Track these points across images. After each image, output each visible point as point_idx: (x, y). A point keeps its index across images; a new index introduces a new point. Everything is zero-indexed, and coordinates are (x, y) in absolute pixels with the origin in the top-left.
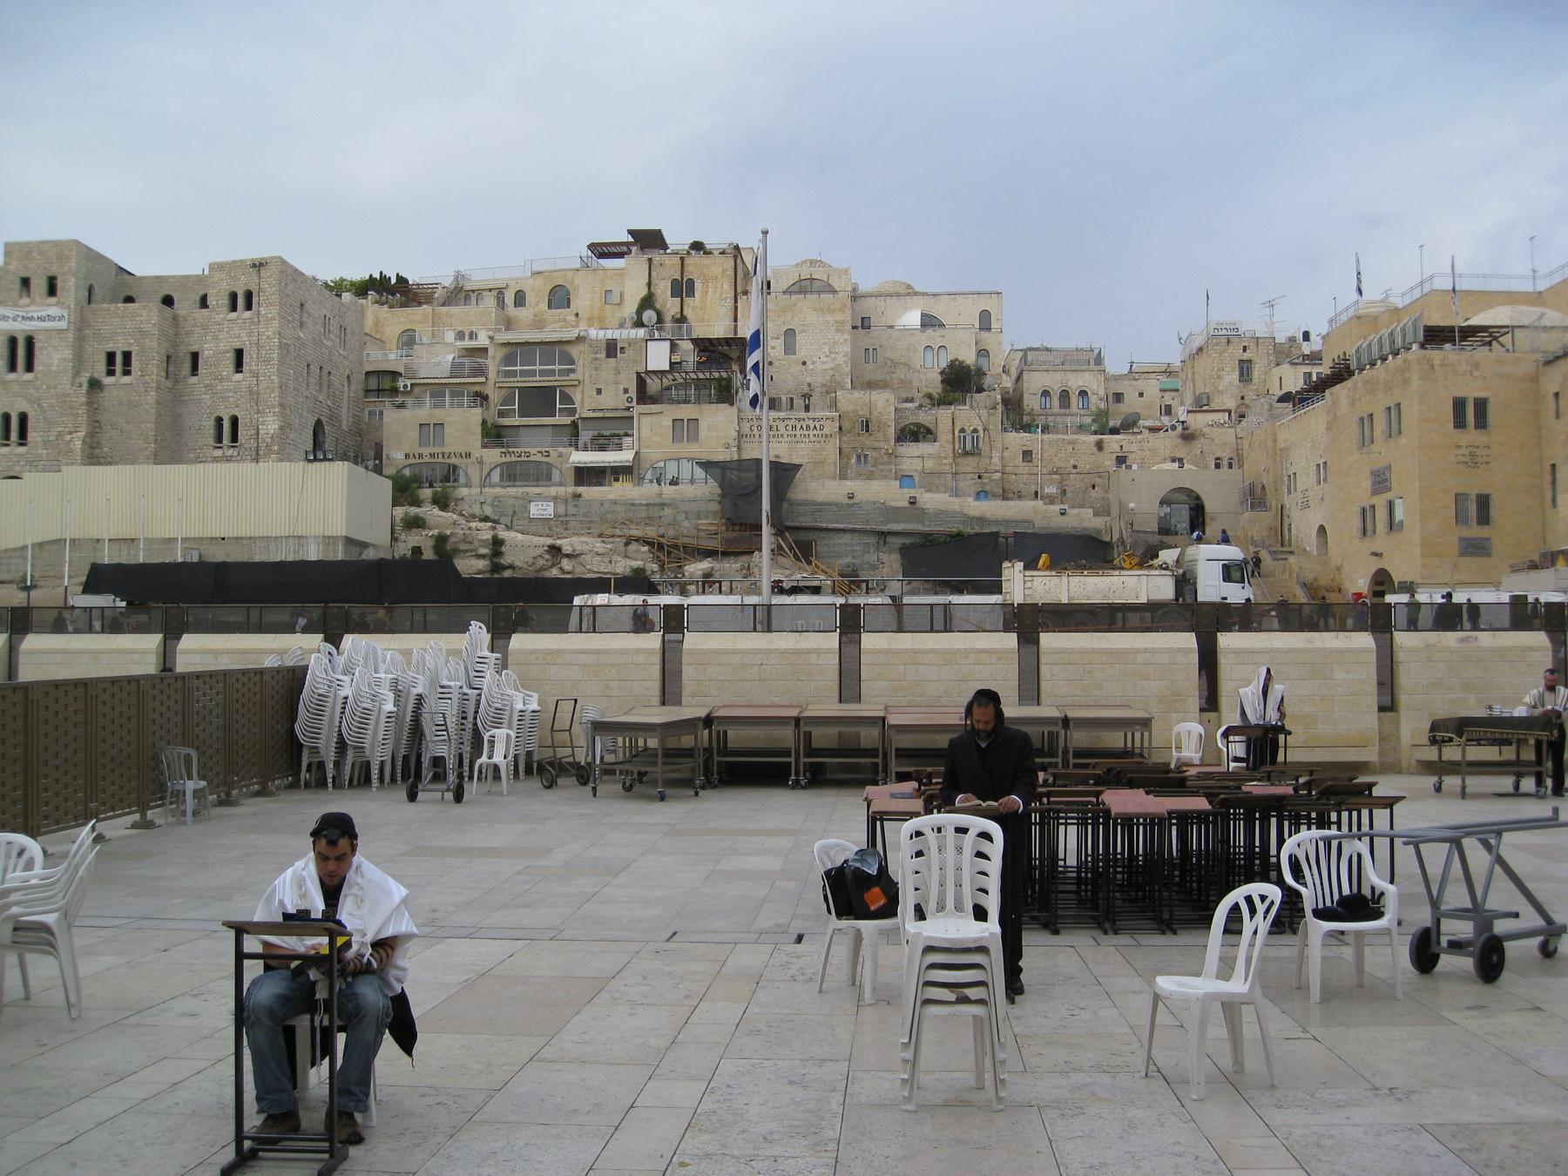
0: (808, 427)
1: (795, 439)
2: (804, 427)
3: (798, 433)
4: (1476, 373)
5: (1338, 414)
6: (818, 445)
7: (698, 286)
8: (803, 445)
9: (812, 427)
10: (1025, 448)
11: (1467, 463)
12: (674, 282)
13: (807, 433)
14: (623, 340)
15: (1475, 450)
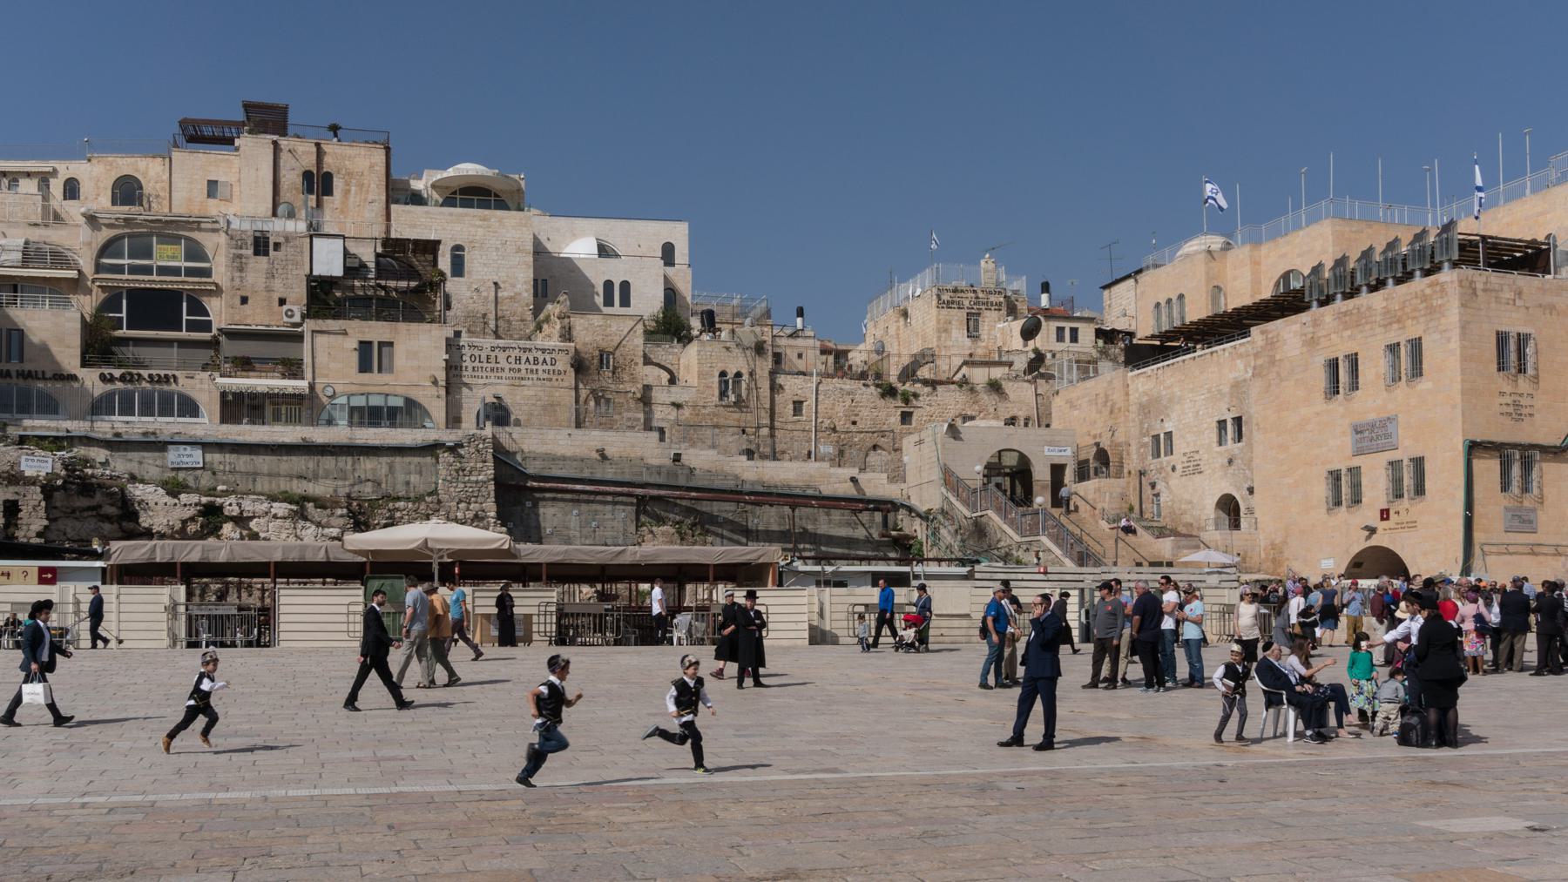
0: (536, 360)
1: (517, 375)
2: (531, 359)
3: (523, 367)
4: (1518, 302)
5: (1278, 357)
6: (547, 383)
7: (338, 183)
8: (530, 382)
9: (541, 360)
10: (796, 398)
11: (1511, 414)
12: (307, 175)
13: (534, 367)
14: (278, 234)
15: (1518, 398)
